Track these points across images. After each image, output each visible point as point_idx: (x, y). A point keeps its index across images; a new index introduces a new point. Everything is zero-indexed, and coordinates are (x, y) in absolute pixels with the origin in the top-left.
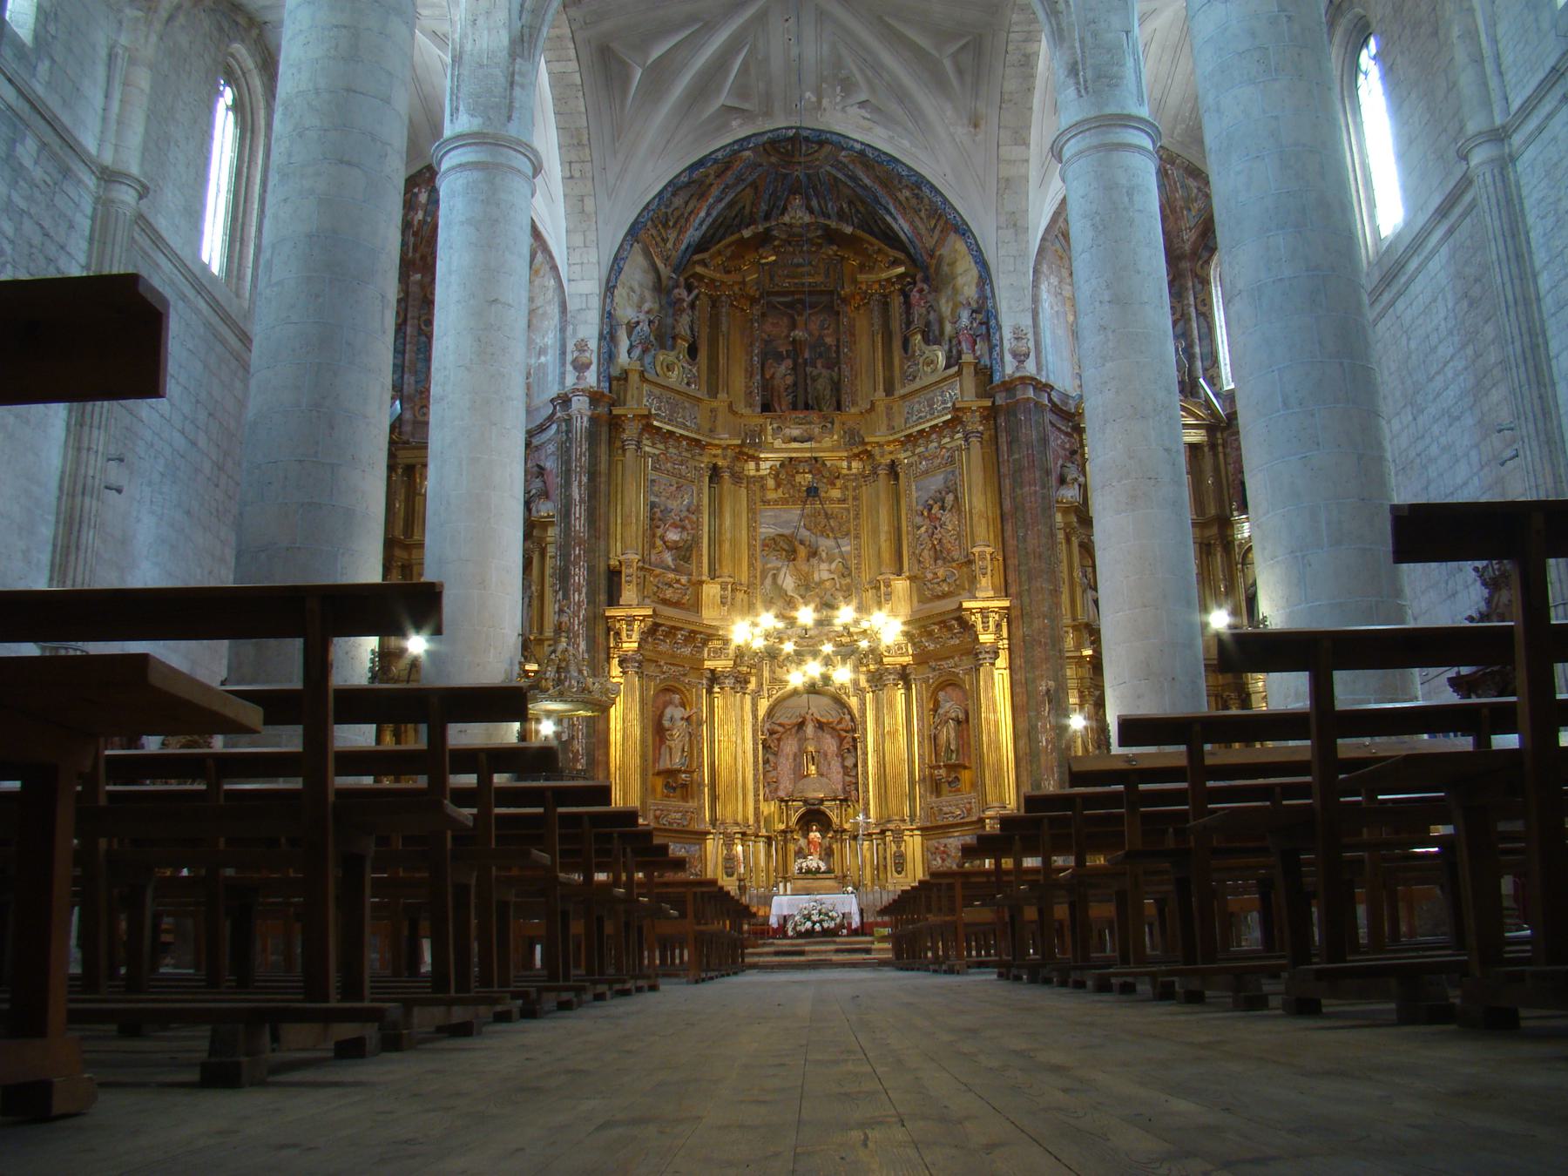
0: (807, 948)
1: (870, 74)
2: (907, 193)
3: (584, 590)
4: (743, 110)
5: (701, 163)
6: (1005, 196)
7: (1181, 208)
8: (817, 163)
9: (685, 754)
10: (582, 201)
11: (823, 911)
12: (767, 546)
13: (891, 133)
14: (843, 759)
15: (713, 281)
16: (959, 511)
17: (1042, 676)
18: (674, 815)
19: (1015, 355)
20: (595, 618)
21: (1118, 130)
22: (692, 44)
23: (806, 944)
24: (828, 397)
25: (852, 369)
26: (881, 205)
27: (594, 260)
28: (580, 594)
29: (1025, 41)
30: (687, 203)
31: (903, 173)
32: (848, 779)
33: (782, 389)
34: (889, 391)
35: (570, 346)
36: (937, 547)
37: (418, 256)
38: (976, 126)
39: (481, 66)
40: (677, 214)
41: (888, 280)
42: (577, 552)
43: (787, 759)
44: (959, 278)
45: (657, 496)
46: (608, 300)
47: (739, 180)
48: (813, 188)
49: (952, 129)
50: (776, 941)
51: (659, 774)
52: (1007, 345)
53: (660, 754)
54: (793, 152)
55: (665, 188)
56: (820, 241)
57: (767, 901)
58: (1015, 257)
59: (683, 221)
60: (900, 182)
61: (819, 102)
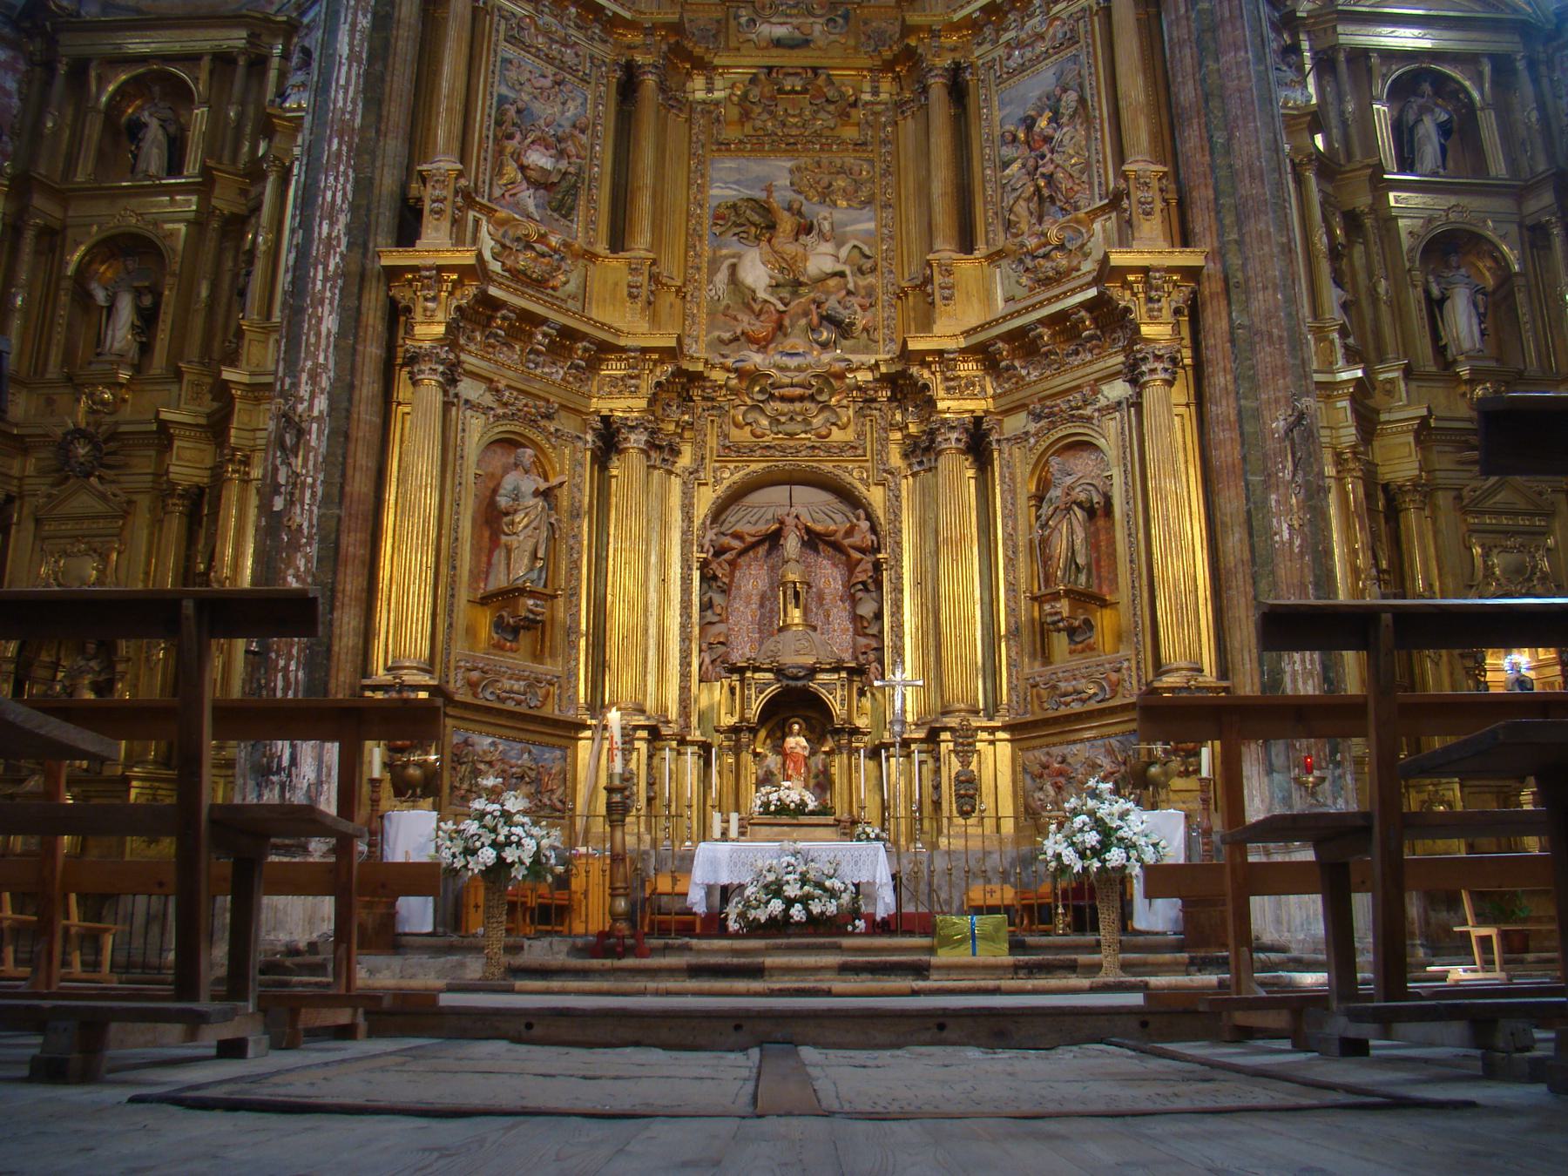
0: (769, 961)
3: (343, 220)
9: (539, 564)
11: (811, 875)
12: (723, 218)
14: (854, 602)
16: (1088, 122)
17: (1277, 401)
18: (507, 684)
20: (363, 277)
23: (767, 951)
28: (332, 225)
32: (862, 641)
36: (1046, 192)
42: (335, 146)
43: (748, 604)
45: (513, 88)
50: (694, 942)
51: (485, 601)
53: (489, 563)
57: (687, 860)
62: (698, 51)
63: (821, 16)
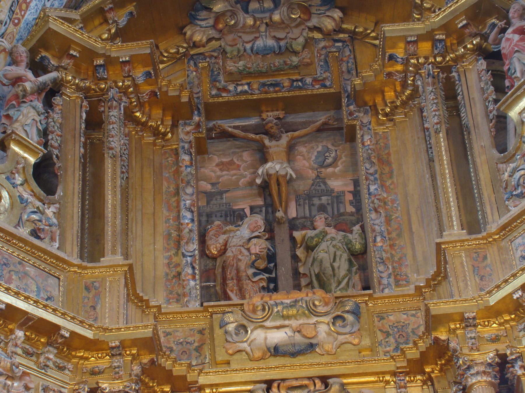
24: (342, 272)
25: (388, 220)
33: (242, 266)
62: (178, 370)
63: (326, 314)
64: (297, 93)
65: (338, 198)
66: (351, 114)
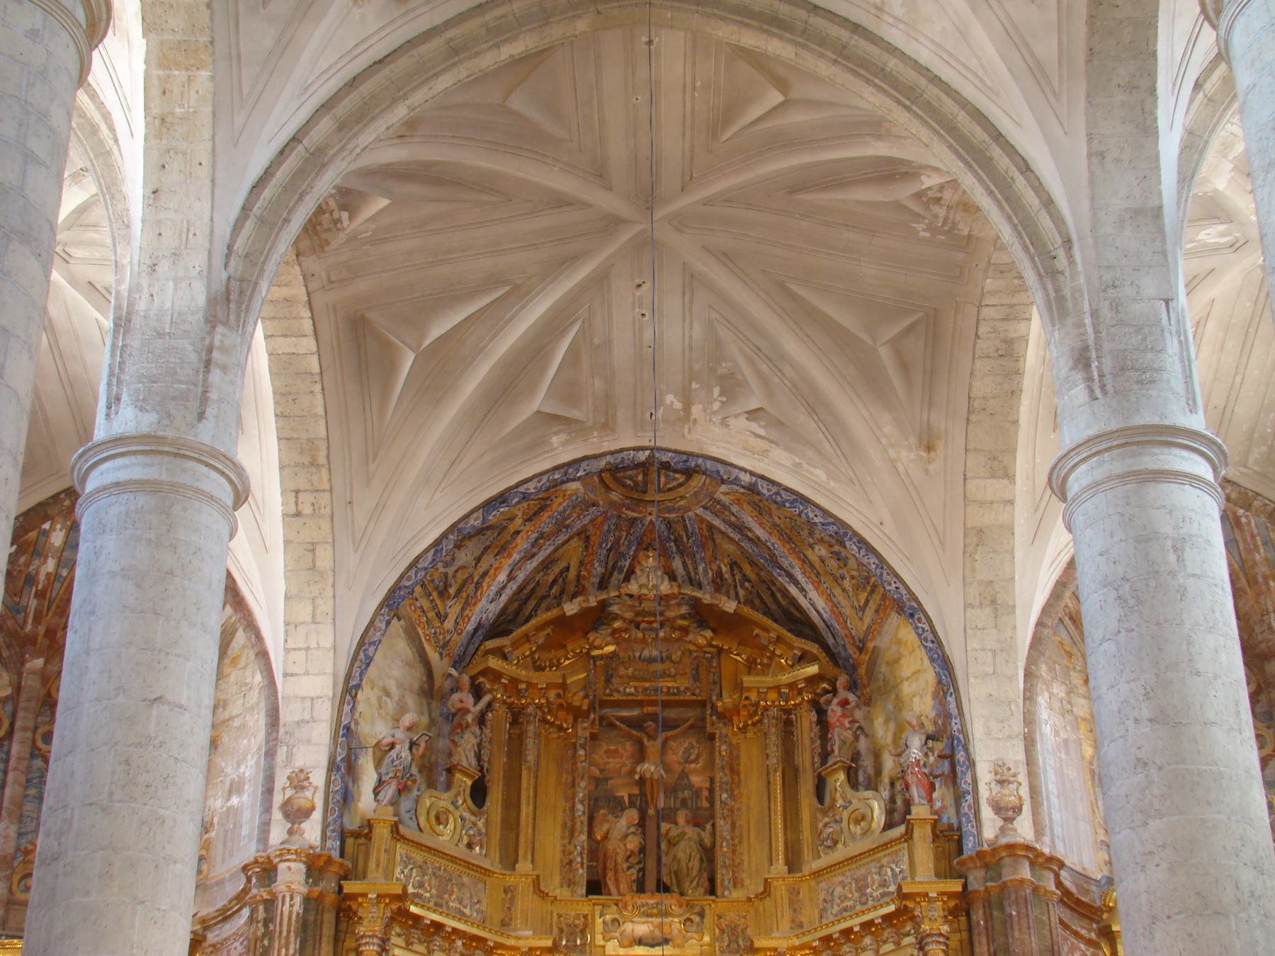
1: (764, 368)
2: (822, 551)
4: (566, 418)
5: (501, 498)
6: (977, 556)
7: (1265, 578)
8: (682, 503)
10: (313, 551)
13: (797, 460)
15: (514, 681)
19: (998, 808)
21: (1156, 450)
22: (493, 318)
24: (695, 873)
25: (733, 826)
26: (781, 568)
27: (327, 641)
29: (1006, 319)
30: (478, 560)
31: (816, 520)
33: (620, 859)
34: (793, 864)
35: (281, 780)
37: (42, 629)
38: (929, 448)
39: (160, 335)
40: (461, 576)
41: (792, 686)
44: (906, 684)
46: (347, 708)
47: (561, 526)
48: (675, 541)
49: (891, 452)
52: (984, 793)
54: (645, 483)
55: (444, 536)
56: (685, 623)
58: (994, 652)
59: (472, 587)
60: (811, 534)
61: (687, 408)
63: (680, 915)
64: (672, 698)
65: (697, 793)
66: (713, 724)
